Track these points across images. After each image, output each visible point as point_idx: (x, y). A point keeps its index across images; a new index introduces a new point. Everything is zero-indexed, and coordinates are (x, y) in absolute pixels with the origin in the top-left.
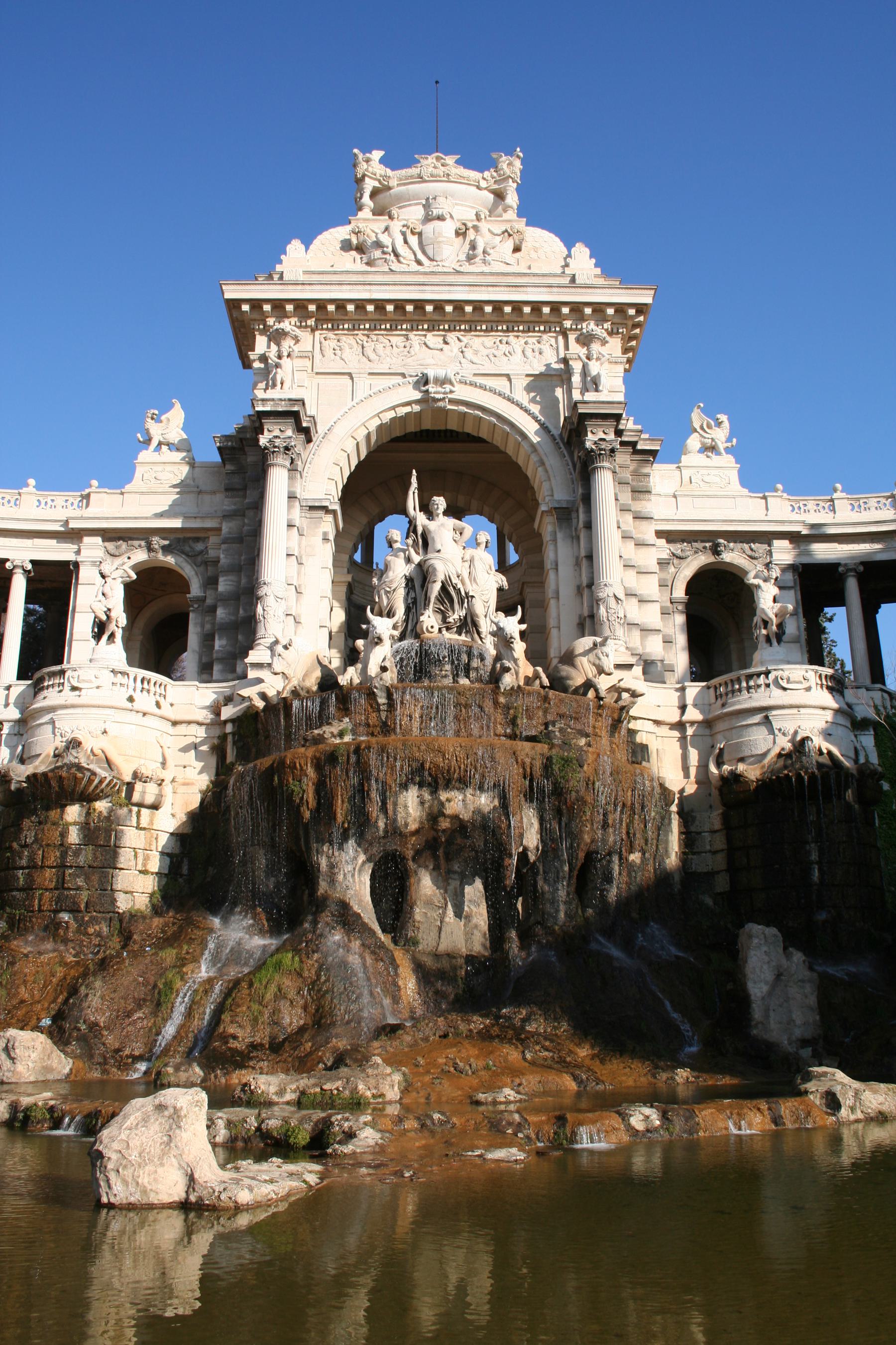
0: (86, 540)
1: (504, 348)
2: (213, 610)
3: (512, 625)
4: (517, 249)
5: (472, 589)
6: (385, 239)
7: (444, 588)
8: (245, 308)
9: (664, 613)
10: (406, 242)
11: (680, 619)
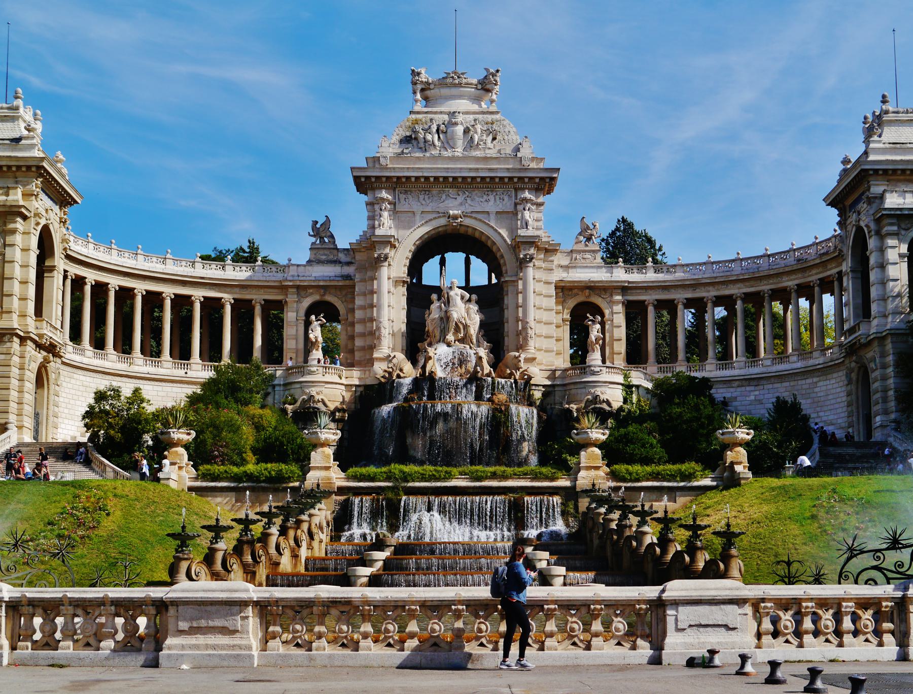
0: (290, 290)
1: (485, 197)
2: (353, 324)
3: (483, 352)
4: (494, 139)
5: (468, 322)
6: (429, 137)
7: (456, 324)
8: (363, 180)
9: (557, 327)
10: (439, 137)
11: (567, 328)
